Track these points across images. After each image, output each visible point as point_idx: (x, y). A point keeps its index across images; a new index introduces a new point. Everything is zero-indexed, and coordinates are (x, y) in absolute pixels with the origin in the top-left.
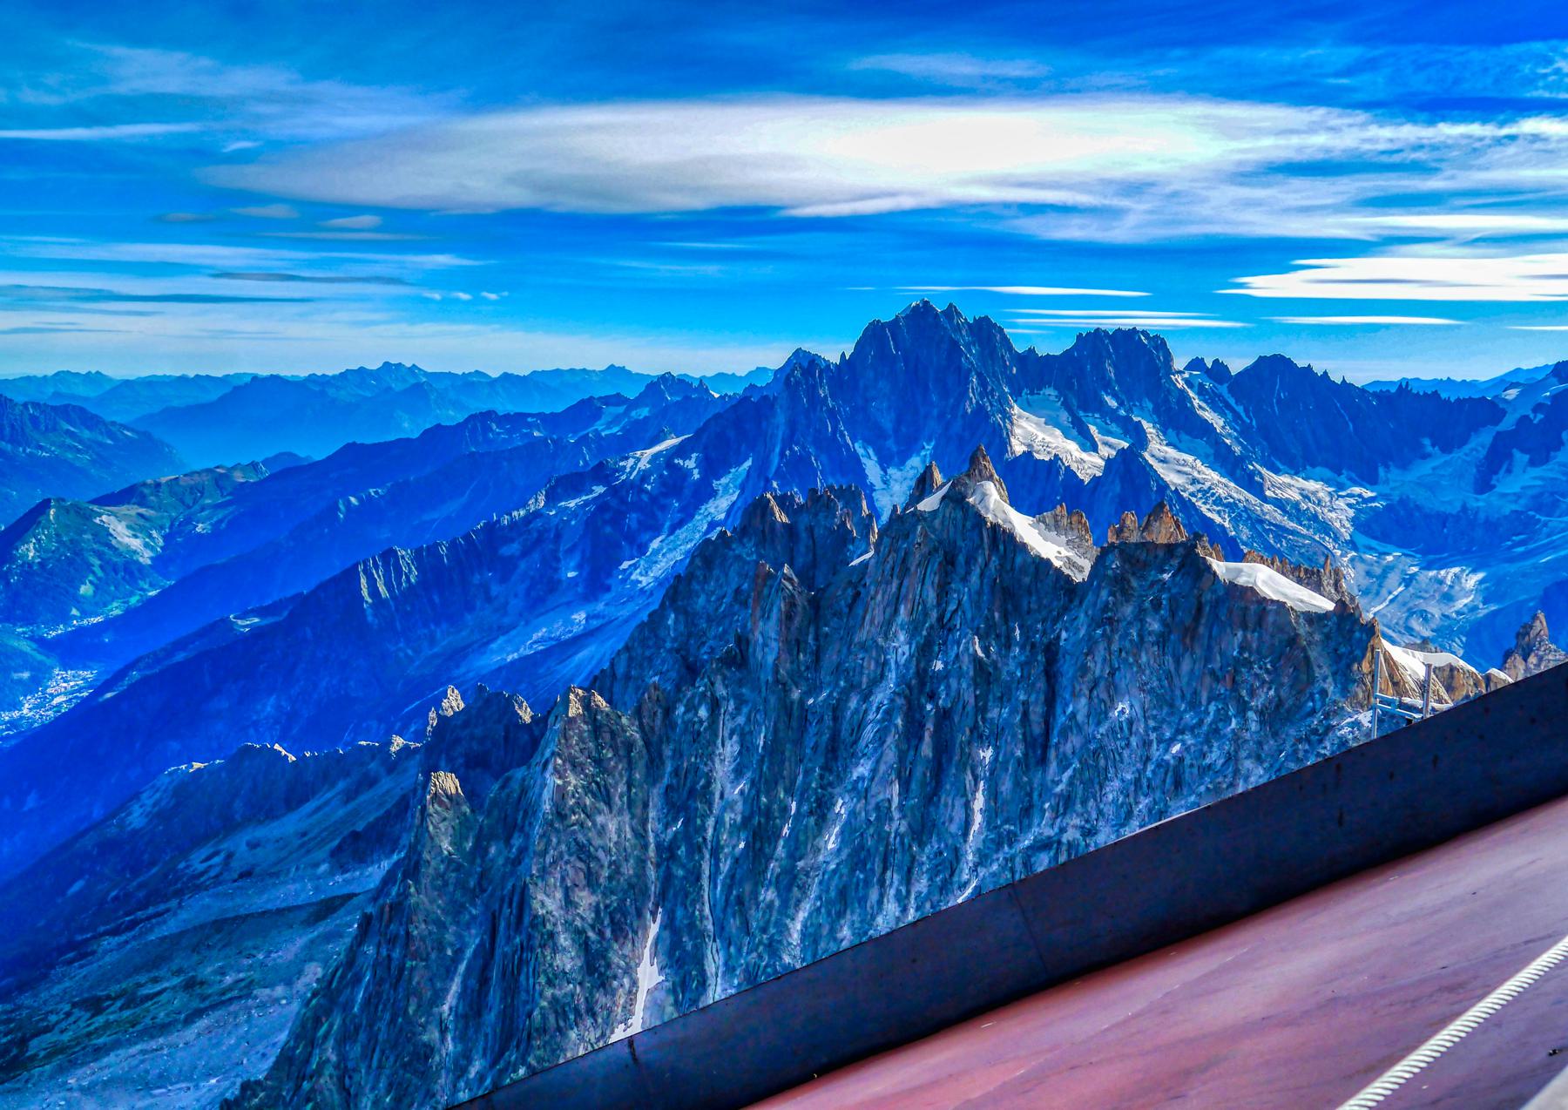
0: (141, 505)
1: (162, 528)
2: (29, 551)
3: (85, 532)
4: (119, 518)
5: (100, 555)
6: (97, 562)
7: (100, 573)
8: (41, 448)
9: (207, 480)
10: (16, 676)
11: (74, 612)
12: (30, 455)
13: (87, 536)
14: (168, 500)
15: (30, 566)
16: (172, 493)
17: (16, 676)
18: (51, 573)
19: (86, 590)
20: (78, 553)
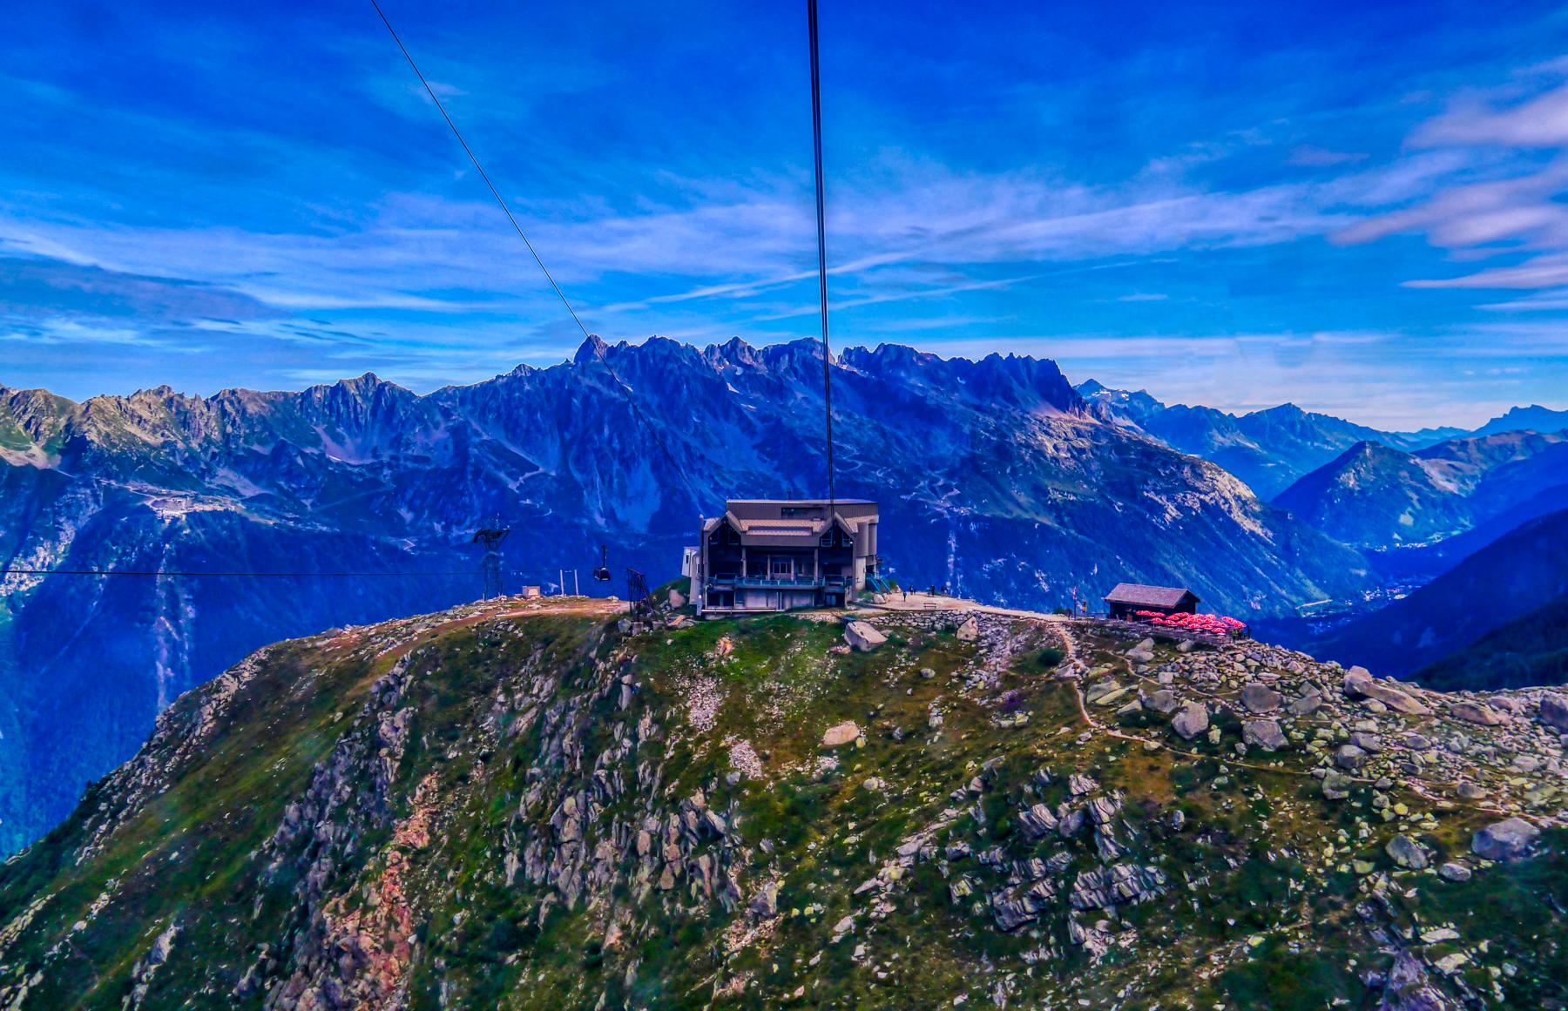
0: (1449, 458)
1: (1473, 478)
2: (1349, 479)
3: (1398, 469)
4: (1432, 466)
5: (1417, 491)
6: (1415, 497)
7: (1418, 507)
8: (1327, 442)
9: (1516, 441)
10: (1354, 571)
11: (1396, 536)
12: (1318, 448)
13: (1404, 473)
14: (1476, 455)
15: (1351, 491)
16: (1479, 449)
17: (1354, 571)
18: (1370, 500)
19: (1406, 519)
20: (1397, 487)
